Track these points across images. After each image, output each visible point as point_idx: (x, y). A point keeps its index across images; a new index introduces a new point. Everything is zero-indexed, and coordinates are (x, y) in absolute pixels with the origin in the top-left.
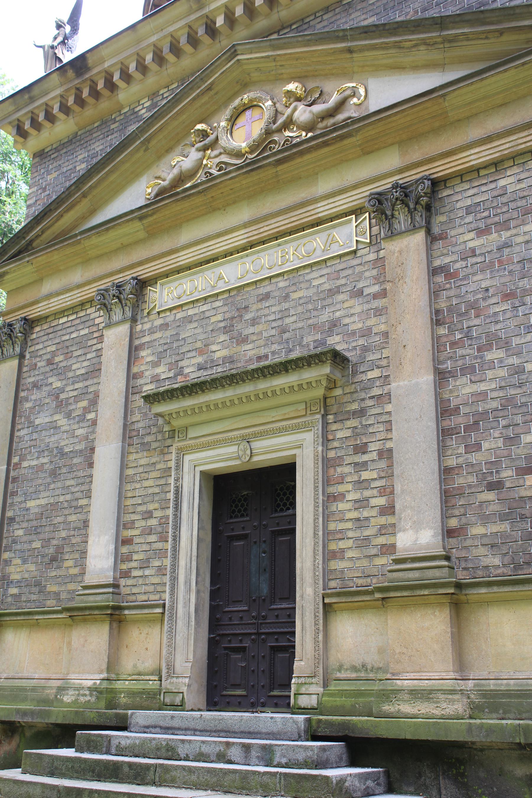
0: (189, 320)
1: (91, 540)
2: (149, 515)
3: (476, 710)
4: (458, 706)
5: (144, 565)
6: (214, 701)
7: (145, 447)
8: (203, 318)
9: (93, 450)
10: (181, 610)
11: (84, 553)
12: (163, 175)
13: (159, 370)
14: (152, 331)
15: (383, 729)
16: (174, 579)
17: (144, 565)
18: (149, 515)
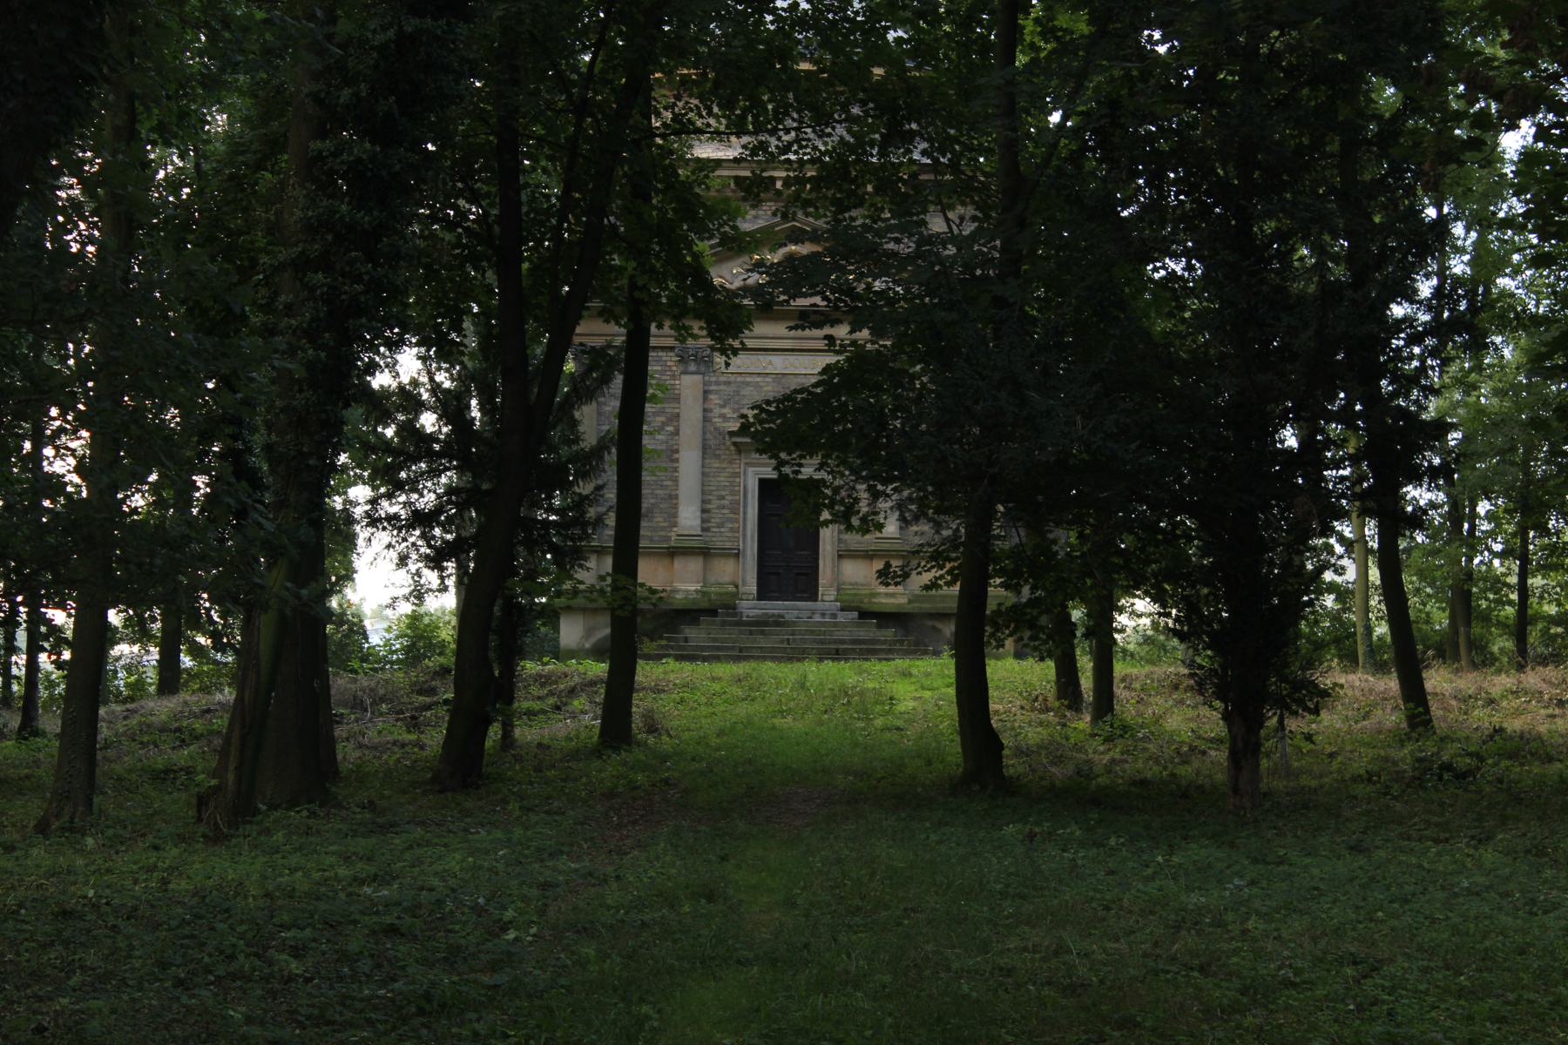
0: (748, 384)
1: (681, 508)
2: (722, 498)
3: (910, 602)
4: (903, 600)
5: (721, 525)
6: (759, 598)
7: (718, 457)
8: (757, 386)
9: (677, 451)
10: (749, 552)
11: (675, 516)
12: (728, 277)
13: (726, 411)
14: (717, 383)
15: (876, 609)
16: (744, 535)
17: (721, 525)
18: (722, 498)
